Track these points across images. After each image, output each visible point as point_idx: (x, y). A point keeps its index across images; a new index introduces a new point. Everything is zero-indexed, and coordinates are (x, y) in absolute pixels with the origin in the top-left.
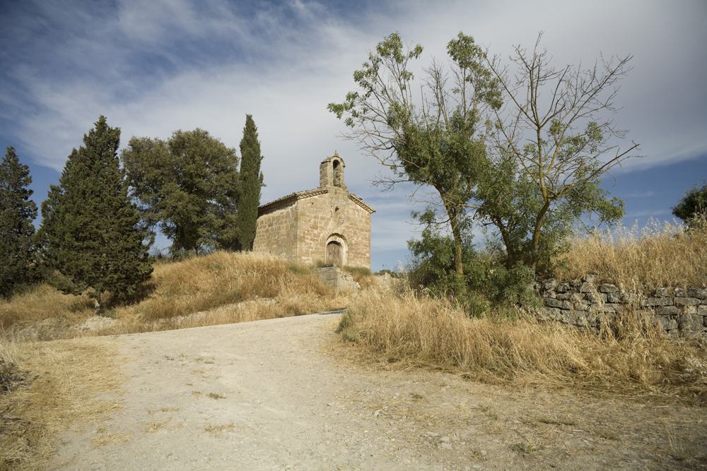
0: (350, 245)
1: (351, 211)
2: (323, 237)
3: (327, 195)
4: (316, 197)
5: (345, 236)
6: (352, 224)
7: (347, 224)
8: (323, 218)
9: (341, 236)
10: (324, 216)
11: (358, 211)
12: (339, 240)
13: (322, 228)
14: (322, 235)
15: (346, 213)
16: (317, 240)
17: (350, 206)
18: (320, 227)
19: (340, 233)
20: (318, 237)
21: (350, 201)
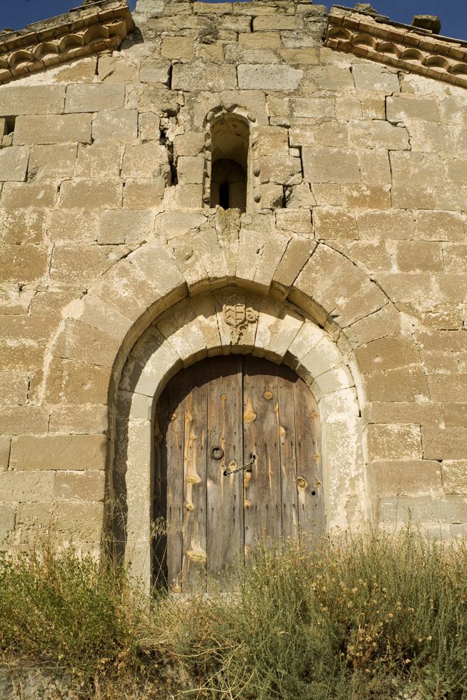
0: (381, 359)
1: (355, 121)
2: (87, 332)
3: (131, 56)
4: (34, 80)
5: (319, 287)
6: (377, 197)
7: (326, 208)
8: (86, 197)
9: (284, 299)
10: (101, 177)
11: (423, 109)
12: (270, 332)
13: (80, 262)
14: (74, 309)
15: (307, 138)
16: (38, 356)
17: (350, 91)
18: (62, 254)
19: (256, 272)
20: (43, 324)
21: (343, 62)
